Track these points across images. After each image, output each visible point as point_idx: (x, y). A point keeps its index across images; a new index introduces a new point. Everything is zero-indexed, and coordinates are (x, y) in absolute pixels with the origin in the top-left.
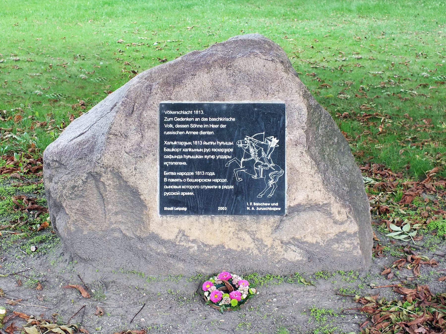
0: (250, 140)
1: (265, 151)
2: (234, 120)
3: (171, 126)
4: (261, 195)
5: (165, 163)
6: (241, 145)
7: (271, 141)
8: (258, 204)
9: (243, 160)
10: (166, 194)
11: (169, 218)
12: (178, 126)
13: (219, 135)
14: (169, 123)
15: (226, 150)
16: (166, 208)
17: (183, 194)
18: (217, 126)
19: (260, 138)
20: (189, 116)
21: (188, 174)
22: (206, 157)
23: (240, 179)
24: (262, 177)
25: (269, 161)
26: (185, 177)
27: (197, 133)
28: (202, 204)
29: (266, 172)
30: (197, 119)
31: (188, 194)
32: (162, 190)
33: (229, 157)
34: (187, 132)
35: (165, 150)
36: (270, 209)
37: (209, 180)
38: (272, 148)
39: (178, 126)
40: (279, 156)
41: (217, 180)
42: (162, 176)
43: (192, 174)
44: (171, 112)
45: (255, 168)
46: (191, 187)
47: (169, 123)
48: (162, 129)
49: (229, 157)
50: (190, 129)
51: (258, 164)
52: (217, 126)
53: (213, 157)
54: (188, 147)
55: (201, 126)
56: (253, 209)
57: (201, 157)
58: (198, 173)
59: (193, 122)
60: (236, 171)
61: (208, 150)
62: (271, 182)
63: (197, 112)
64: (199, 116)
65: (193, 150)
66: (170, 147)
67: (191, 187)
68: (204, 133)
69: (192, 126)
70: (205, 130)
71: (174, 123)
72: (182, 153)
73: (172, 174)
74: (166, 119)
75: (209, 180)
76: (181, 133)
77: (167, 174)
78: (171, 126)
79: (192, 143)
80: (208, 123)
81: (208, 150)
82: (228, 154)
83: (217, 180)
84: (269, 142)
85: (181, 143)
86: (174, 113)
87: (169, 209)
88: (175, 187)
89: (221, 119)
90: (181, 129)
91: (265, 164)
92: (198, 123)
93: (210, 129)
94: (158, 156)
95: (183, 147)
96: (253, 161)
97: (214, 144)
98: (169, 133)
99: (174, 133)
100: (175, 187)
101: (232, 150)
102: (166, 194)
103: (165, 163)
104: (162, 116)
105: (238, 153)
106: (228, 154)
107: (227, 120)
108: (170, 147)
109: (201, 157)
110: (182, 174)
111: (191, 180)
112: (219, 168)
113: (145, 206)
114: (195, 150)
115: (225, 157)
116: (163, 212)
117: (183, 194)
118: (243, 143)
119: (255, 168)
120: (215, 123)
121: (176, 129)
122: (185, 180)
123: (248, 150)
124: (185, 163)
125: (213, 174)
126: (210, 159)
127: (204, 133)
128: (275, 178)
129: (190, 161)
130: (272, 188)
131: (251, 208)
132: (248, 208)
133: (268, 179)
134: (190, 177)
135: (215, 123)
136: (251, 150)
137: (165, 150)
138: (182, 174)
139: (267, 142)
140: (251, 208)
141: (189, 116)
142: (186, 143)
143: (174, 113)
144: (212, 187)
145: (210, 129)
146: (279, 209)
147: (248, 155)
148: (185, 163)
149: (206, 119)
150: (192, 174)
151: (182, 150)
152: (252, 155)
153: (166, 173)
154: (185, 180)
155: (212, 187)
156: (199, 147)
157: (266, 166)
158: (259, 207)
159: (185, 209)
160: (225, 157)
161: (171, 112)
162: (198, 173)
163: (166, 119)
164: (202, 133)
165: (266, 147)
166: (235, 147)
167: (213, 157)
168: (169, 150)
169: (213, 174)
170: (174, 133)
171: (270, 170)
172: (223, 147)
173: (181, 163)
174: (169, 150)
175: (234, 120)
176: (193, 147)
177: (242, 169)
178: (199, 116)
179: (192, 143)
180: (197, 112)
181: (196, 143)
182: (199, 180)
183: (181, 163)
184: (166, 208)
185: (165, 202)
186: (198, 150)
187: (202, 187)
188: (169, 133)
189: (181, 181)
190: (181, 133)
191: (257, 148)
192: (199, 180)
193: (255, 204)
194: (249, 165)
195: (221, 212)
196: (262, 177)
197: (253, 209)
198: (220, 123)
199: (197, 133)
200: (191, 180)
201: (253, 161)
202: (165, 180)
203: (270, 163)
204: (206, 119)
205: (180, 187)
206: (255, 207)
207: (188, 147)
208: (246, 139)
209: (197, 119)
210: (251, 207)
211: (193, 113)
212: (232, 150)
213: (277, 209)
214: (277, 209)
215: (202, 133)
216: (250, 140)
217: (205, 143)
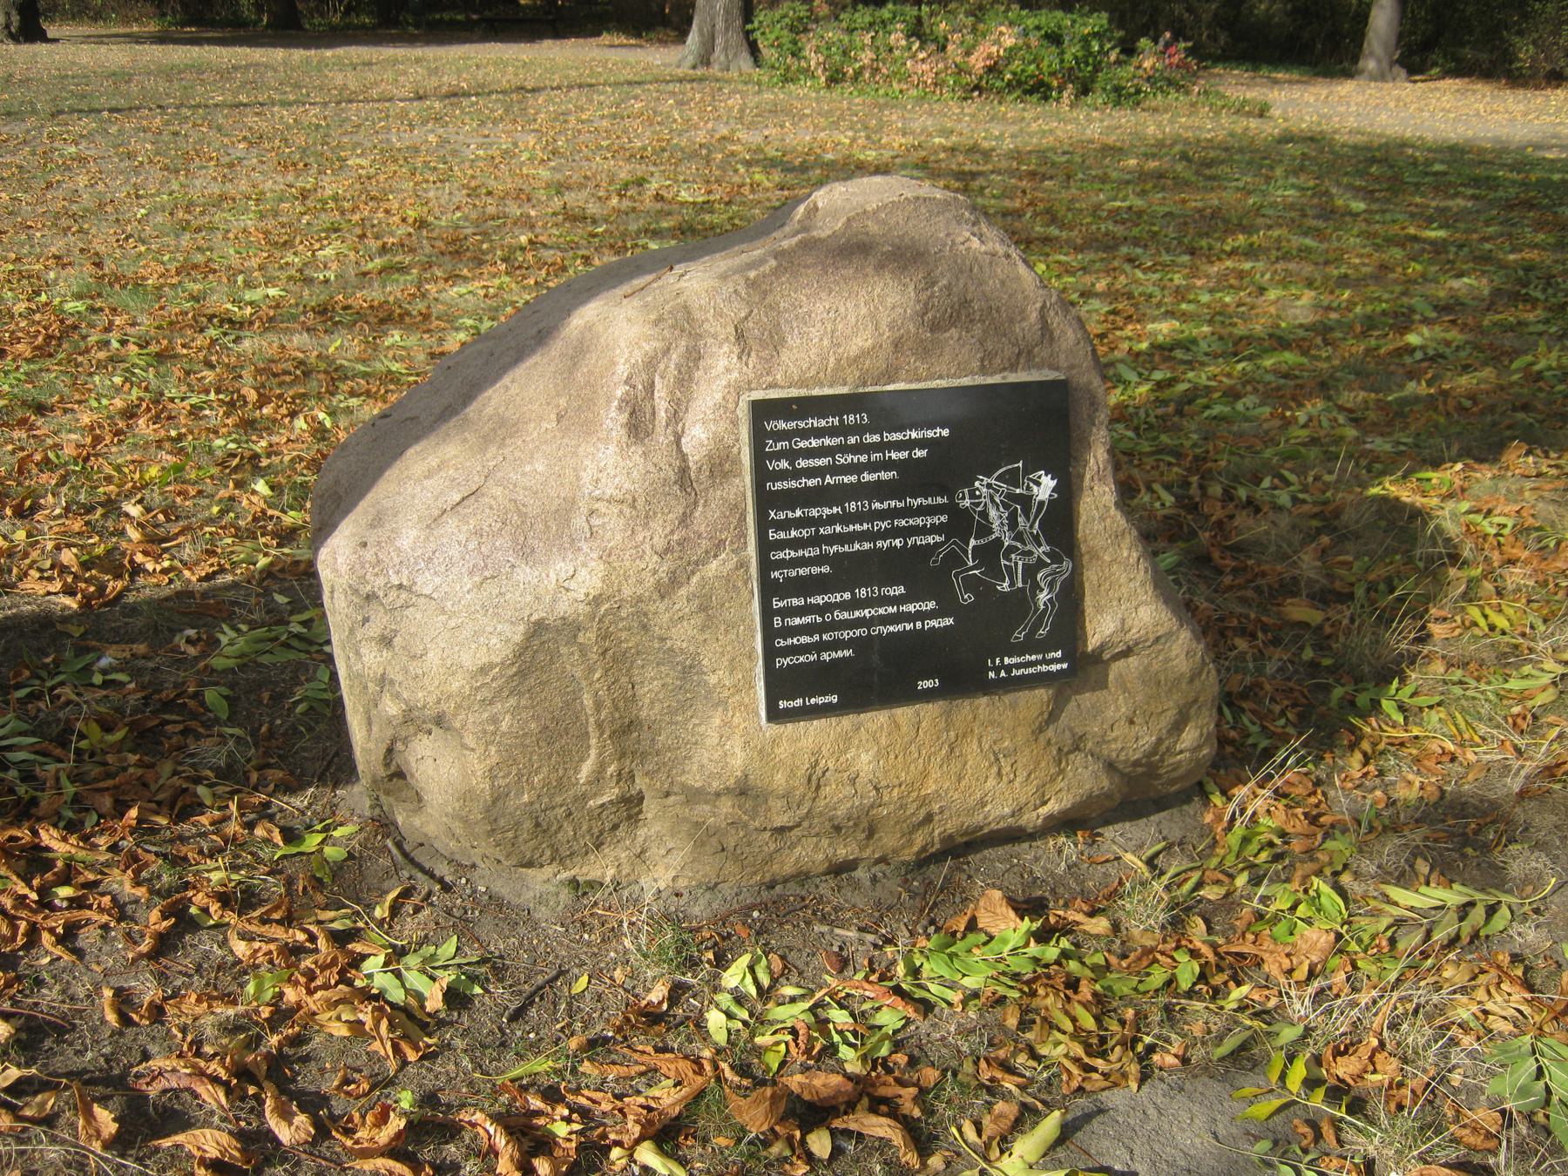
0: (989, 486)
1: (1026, 514)
2: (945, 433)
3: (784, 464)
4: (1020, 635)
6: (967, 503)
7: (1038, 484)
8: (1014, 660)
9: (972, 542)
10: (783, 662)
12: (802, 463)
13: (913, 479)
16: (782, 704)
17: (826, 656)
18: (904, 455)
19: (1012, 478)
20: (831, 432)
21: (837, 598)
22: (879, 544)
23: (968, 598)
24: (1020, 585)
25: (1036, 539)
26: (829, 607)
27: (853, 479)
28: (872, 679)
29: (1030, 571)
30: (852, 440)
31: (840, 654)
32: (770, 653)
33: (938, 539)
34: (828, 479)
35: (772, 535)
36: (1044, 668)
37: (892, 610)
38: (1041, 503)
39: (802, 463)
40: (1060, 523)
42: (767, 613)
43: (847, 596)
44: (782, 425)
45: (1003, 562)
46: (846, 635)
48: (761, 475)
49: (938, 539)
50: (835, 470)
51: (1012, 549)
52: (904, 455)
53: (898, 543)
54: (832, 520)
55: (863, 458)
56: (1003, 674)
57: (867, 546)
58: (863, 593)
59: (844, 449)
60: (956, 576)
61: (884, 525)
62: (1043, 597)
63: (851, 419)
64: (859, 430)
65: (846, 530)
66: (785, 525)
67: (846, 635)
68: (873, 477)
69: (841, 460)
70: (873, 467)
71: (792, 455)
72: (816, 541)
73: (795, 602)
74: (771, 446)
75: (892, 610)
76: (812, 483)
77: (781, 604)
78: (784, 464)
79: (844, 509)
80: (882, 447)
81: (884, 525)
82: (934, 530)
84: (1035, 488)
85: (814, 513)
86: (792, 425)
87: (791, 704)
88: (805, 639)
89: (914, 435)
90: (811, 473)
91: (1028, 548)
92: (856, 449)
93: (887, 465)
94: (752, 550)
95: (819, 522)
96: (999, 542)
97: (901, 505)
98: (779, 486)
99: (793, 484)
100: (805, 639)
101: (944, 518)
102: (783, 662)
105: (962, 523)
106: (934, 530)
107: (930, 434)
108: (785, 525)
109: (867, 546)
110: (819, 600)
111: (846, 615)
112: (914, 570)
114: (851, 527)
115: (930, 540)
116: (774, 715)
117: (826, 656)
118: (972, 495)
119: (1003, 562)
121: (796, 474)
122: (828, 617)
123: (984, 514)
124: (826, 569)
125: (899, 590)
126: (891, 549)
127: (873, 477)
128: (1051, 585)
130: (1045, 610)
131: (998, 674)
132: (992, 675)
133: (1036, 587)
134: (843, 606)
135: (898, 446)
136: (993, 513)
137: (772, 535)
138: (819, 600)
139: (1028, 488)
140: (998, 674)
142: (827, 511)
143: (792, 425)
144: (900, 627)
145: (887, 465)
146: (1065, 666)
147: (985, 530)
148: (826, 569)
149: (876, 438)
150: (847, 596)
151: (817, 531)
152: (996, 526)
153: (777, 604)
154: (828, 617)
155: (900, 627)
157: (1030, 553)
158: (1018, 666)
159: (834, 699)
160: (930, 540)
161: (782, 425)
162: (863, 593)
163: (771, 446)
164: (867, 477)
165: (1026, 501)
166: (952, 509)
167: (898, 543)
168: (782, 535)
169: (899, 590)
170: (793, 484)
171: (1041, 564)
173: (815, 570)
174: (782, 535)
175: (945, 433)
176: (846, 519)
177: (972, 568)
178: (859, 430)
179: (844, 509)
180: (851, 419)
181: (852, 506)
182: (866, 613)
183: (815, 570)
184: (782, 704)
185: (780, 684)
186: (858, 527)
188: (779, 486)
189: (819, 620)
190: (812, 483)
191: (1006, 506)
192: (866, 613)
193: (1007, 661)
194: (990, 554)
195: (928, 696)
196: (1020, 585)
197: (1003, 674)
198: (910, 445)
199: (853, 479)
200: (846, 615)
201: (999, 542)
202: (777, 622)
203: (1040, 545)
204: (876, 438)
205: (816, 638)
206: (1009, 668)
207: (832, 520)
208: (977, 484)
209: (852, 440)
210: (997, 670)
211: (842, 421)
212: (944, 518)
213: (1059, 666)
214: (1059, 666)
215: (867, 477)
216: (989, 486)
217: (877, 505)
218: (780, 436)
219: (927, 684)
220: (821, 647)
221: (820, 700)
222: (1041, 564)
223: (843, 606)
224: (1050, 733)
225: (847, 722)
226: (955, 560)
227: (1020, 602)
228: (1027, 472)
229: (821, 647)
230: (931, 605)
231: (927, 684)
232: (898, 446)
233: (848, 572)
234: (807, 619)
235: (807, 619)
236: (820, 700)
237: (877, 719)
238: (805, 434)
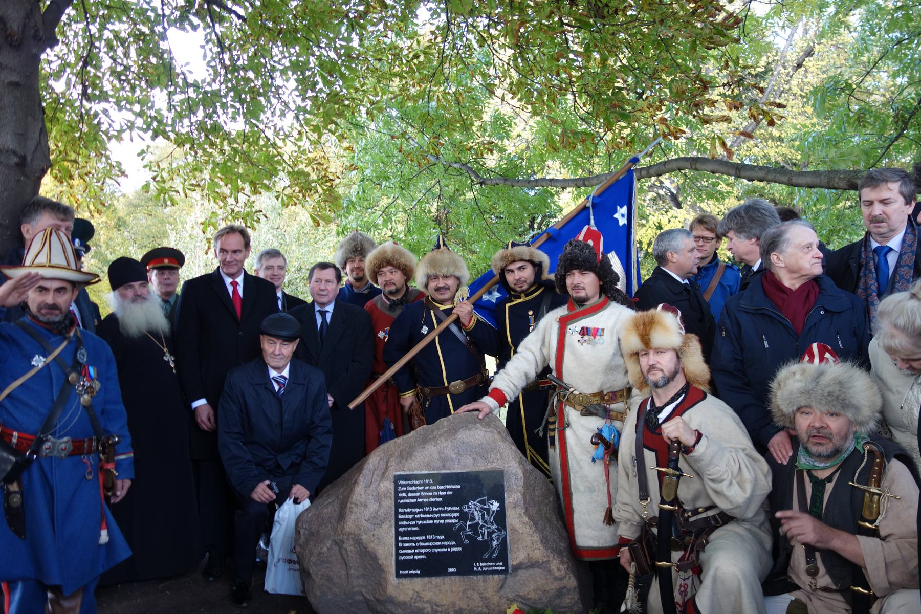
1: (488, 514)
3: (404, 495)
4: (486, 556)
5: (400, 529)
6: (467, 510)
10: (401, 558)
11: (405, 581)
12: (410, 495)
13: (447, 501)
14: (402, 492)
15: (453, 515)
16: (401, 572)
17: (416, 557)
18: (444, 493)
19: (483, 502)
20: (420, 485)
21: (420, 538)
23: (467, 542)
25: (492, 523)
26: (418, 541)
30: (427, 488)
32: (398, 555)
35: (400, 517)
37: (439, 544)
39: (410, 495)
40: (500, 518)
41: (446, 543)
42: (397, 541)
44: (404, 482)
46: (423, 551)
47: (402, 492)
48: (397, 498)
51: (483, 526)
52: (444, 493)
54: (419, 513)
57: (431, 522)
58: (429, 537)
59: (424, 490)
62: (495, 543)
63: (426, 481)
64: (429, 485)
66: (404, 514)
67: (423, 551)
68: (433, 500)
69: (423, 494)
70: (433, 497)
71: (407, 492)
72: (414, 519)
74: (400, 489)
75: (439, 544)
76: (413, 501)
78: (404, 495)
80: (437, 490)
82: (454, 518)
83: (446, 543)
85: (414, 510)
88: (409, 551)
90: (413, 498)
92: (428, 491)
93: (439, 496)
94: (393, 522)
95: (415, 513)
96: (478, 523)
98: (402, 501)
99: (407, 501)
100: (409, 551)
101: (458, 514)
102: (401, 558)
103: (400, 529)
104: (397, 486)
105: (464, 517)
106: (454, 518)
108: (404, 514)
109: (431, 522)
110: (414, 538)
111: (423, 544)
113: (383, 570)
115: (453, 521)
116: (398, 575)
117: (416, 557)
120: (443, 490)
121: (408, 498)
123: (473, 514)
124: (417, 529)
125: (443, 537)
126: (439, 524)
128: (498, 540)
129: (420, 526)
133: (492, 540)
134: (423, 541)
135: (443, 490)
136: (476, 514)
137: (400, 517)
138: (414, 538)
141: (420, 485)
142: (418, 510)
145: (439, 496)
147: (473, 519)
148: (417, 529)
153: (400, 539)
156: (429, 512)
159: (419, 572)
161: (404, 482)
162: (429, 537)
163: (400, 489)
165: (488, 510)
166: (461, 511)
168: (403, 517)
169: (443, 537)
170: (407, 501)
171: (494, 532)
172: (450, 512)
173: (413, 529)
174: (403, 517)
176: (425, 513)
178: (429, 485)
180: (426, 481)
181: (426, 509)
182: (431, 544)
183: (413, 529)
184: (401, 572)
185: (400, 565)
187: (433, 550)
188: (402, 501)
190: (413, 501)
192: (431, 544)
194: (475, 527)
195: (452, 574)
198: (447, 490)
200: (423, 544)
201: (478, 523)
202: (400, 545)
206: (482, 567)
207: (419, 513)
209: (427, 488)
212: (458, 514)
215: (432, 500)
218: (402, 486)
219: (450, 570)
220: (414, 554)
221: (414, 572)
222: (494, 532)
223: (423, 541)
224: (502, 593)
225: (426, 579)
226: (462, 528)
227: (486, 545)
228: (489, 500)
229: (414, 554)
230: (453, 543)
231: (450, 570)
232: (439, 490)
233: (424, 530)
234: (410, 545)
235: (410, 545)
236: (414, 572)
237: (435, 580)
238: (411, 485)
